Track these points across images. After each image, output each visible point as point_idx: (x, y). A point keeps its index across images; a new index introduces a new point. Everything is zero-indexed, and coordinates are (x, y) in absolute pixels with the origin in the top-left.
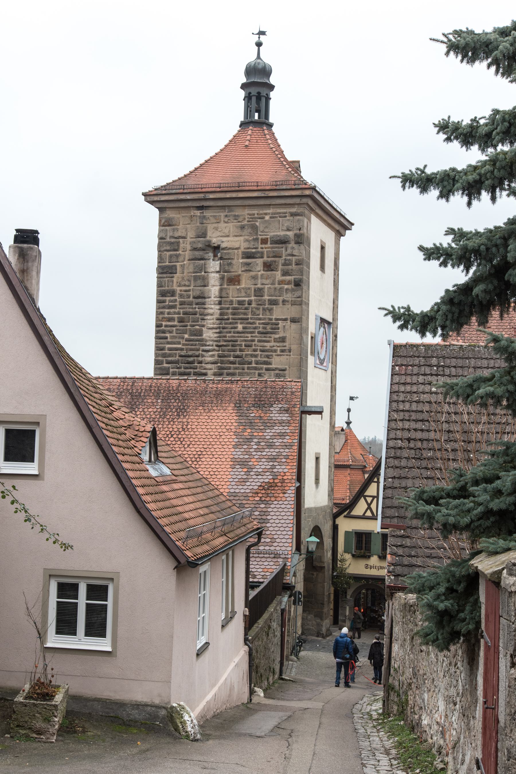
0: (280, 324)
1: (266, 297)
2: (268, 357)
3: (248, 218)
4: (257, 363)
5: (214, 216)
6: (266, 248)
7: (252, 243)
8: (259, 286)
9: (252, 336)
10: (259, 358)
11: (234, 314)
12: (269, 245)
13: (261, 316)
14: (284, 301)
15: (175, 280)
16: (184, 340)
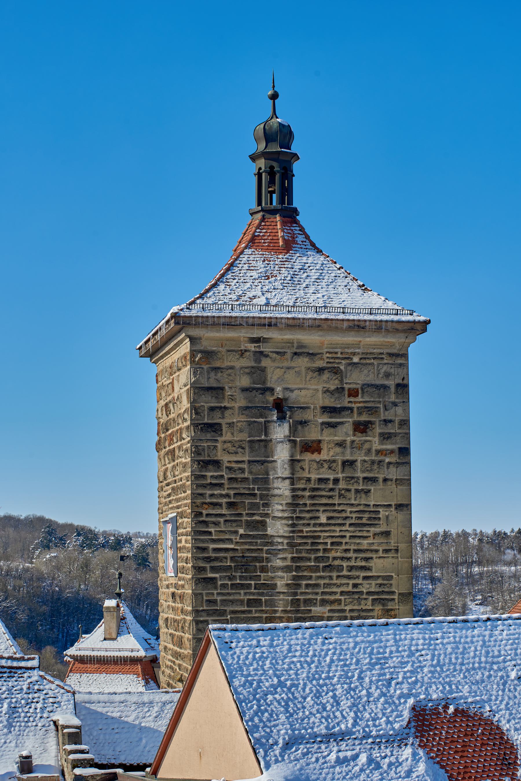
0: (382, 513)
1: (361, 475)
2: (367, 559)
3: (328, 358)
4: (351, 568)
5: (277, 353)
6: (355, 402)
7: (337, 395)
8: (348, 457)
9: (341, 531)
10: (352, 563)
11: (312, 497)
12: (359, 399)
13: (353, 502)
14: (385, 480)
15: (219, 445)
16: (238, 538)
